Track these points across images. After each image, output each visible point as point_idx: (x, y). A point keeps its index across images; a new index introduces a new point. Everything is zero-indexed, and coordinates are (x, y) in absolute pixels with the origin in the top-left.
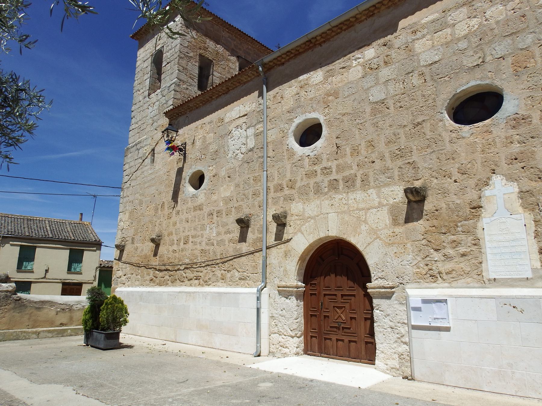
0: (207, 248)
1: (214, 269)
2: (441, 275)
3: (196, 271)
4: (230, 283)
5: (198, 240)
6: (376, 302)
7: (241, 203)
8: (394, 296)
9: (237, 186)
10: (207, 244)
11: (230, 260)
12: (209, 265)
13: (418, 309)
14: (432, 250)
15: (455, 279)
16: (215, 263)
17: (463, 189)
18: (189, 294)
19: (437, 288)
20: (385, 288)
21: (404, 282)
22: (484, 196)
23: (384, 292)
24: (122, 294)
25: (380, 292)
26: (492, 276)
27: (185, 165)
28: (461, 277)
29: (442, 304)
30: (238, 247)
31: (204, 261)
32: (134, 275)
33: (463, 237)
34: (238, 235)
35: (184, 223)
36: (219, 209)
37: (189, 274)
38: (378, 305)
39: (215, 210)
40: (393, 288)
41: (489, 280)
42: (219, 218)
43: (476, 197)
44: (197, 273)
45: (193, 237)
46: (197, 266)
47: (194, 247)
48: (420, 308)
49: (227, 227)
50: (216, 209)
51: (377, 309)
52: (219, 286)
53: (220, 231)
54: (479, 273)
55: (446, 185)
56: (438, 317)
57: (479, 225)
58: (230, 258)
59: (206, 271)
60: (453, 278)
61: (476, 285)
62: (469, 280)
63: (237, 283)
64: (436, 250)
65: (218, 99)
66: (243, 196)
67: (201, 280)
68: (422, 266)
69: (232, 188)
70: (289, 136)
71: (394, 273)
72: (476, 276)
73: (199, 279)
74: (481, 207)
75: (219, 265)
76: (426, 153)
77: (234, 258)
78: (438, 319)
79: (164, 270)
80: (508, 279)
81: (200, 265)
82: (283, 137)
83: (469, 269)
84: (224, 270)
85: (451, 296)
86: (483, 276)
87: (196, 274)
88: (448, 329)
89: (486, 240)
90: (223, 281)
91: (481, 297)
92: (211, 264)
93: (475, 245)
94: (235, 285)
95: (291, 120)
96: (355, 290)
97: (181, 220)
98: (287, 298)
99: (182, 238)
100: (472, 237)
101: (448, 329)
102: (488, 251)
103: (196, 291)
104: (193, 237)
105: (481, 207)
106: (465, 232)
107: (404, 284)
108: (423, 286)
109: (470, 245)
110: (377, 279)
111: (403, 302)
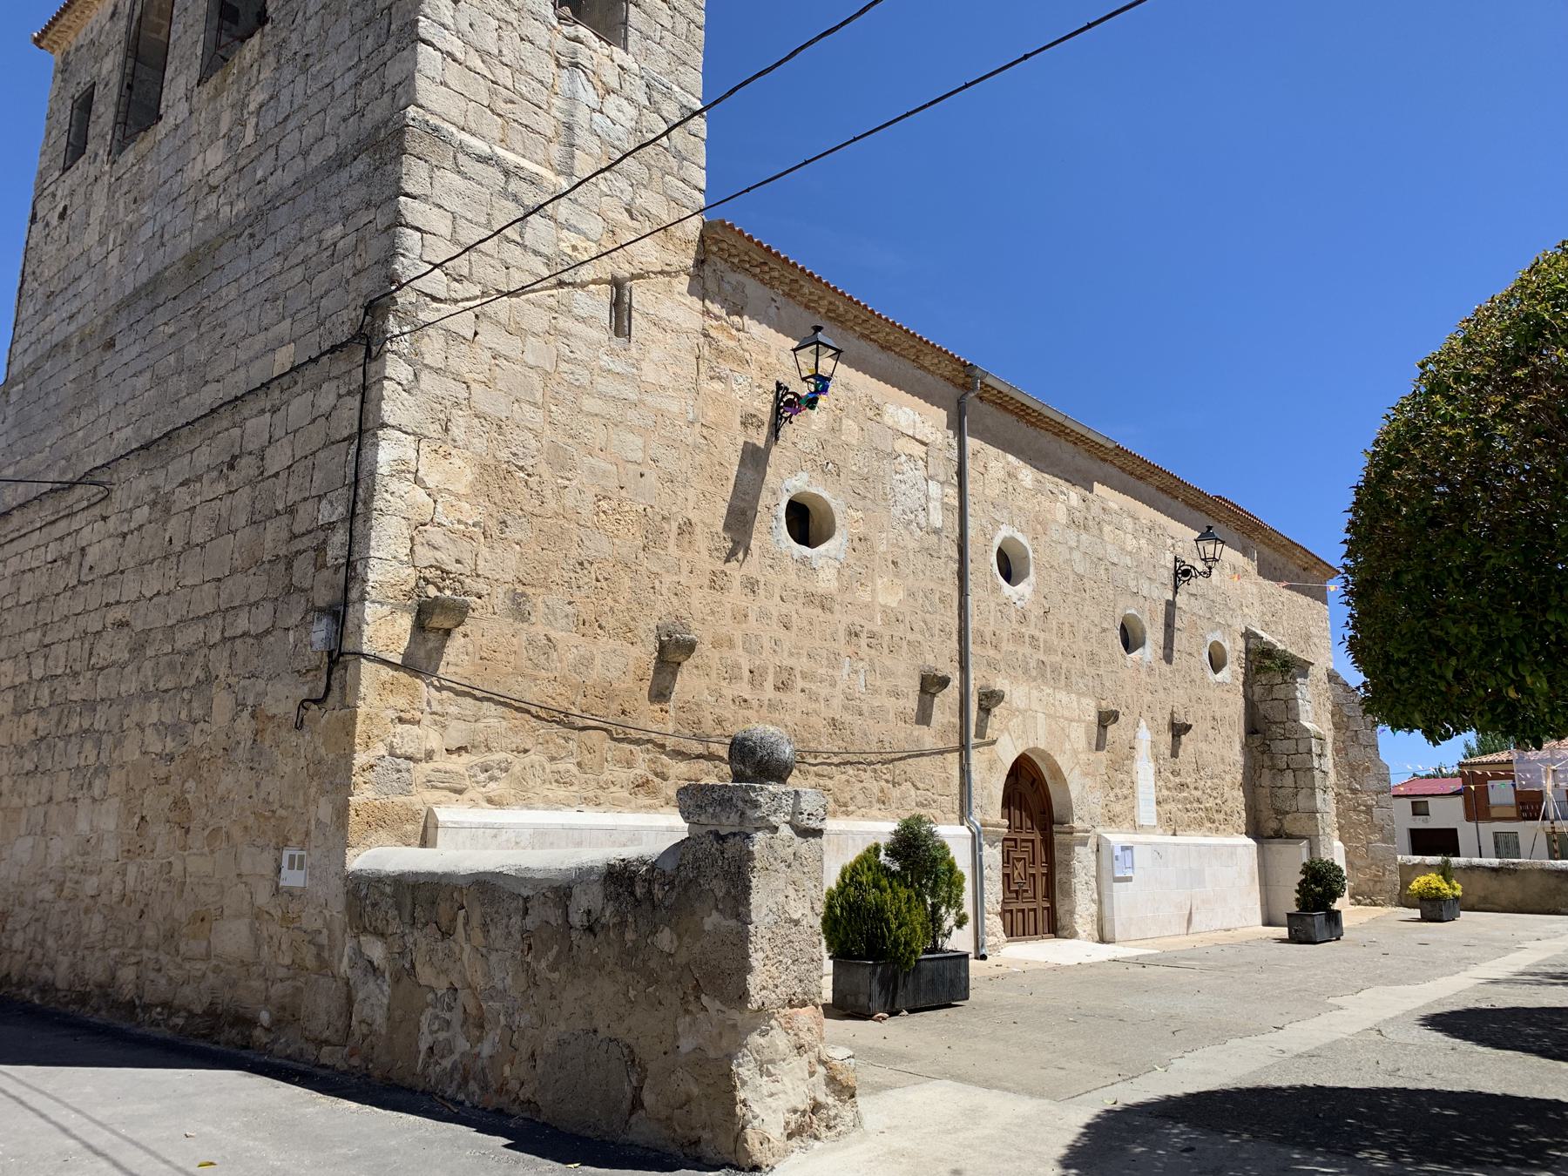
3: (817, 775)
9: (912, 594)
11: (900, 759)
12: (851, 764)
24: (495, 836)
27: (774, 450)
30: (916, 733)
32: (532, 757)
34: (916, 708)
35: (775, 627)
45: (804, 676)
46: (818, 761)
47: (812, 706)
52: (875, 819)
58: (900, 755)
65: (863, 343)
77: (910, 757)
79: (699, 757)
84: (887, 781)
88: (1129, 879)
97: (764, 615)
99: (771, 671)
101: (1129, 879)
104: (804, 676)
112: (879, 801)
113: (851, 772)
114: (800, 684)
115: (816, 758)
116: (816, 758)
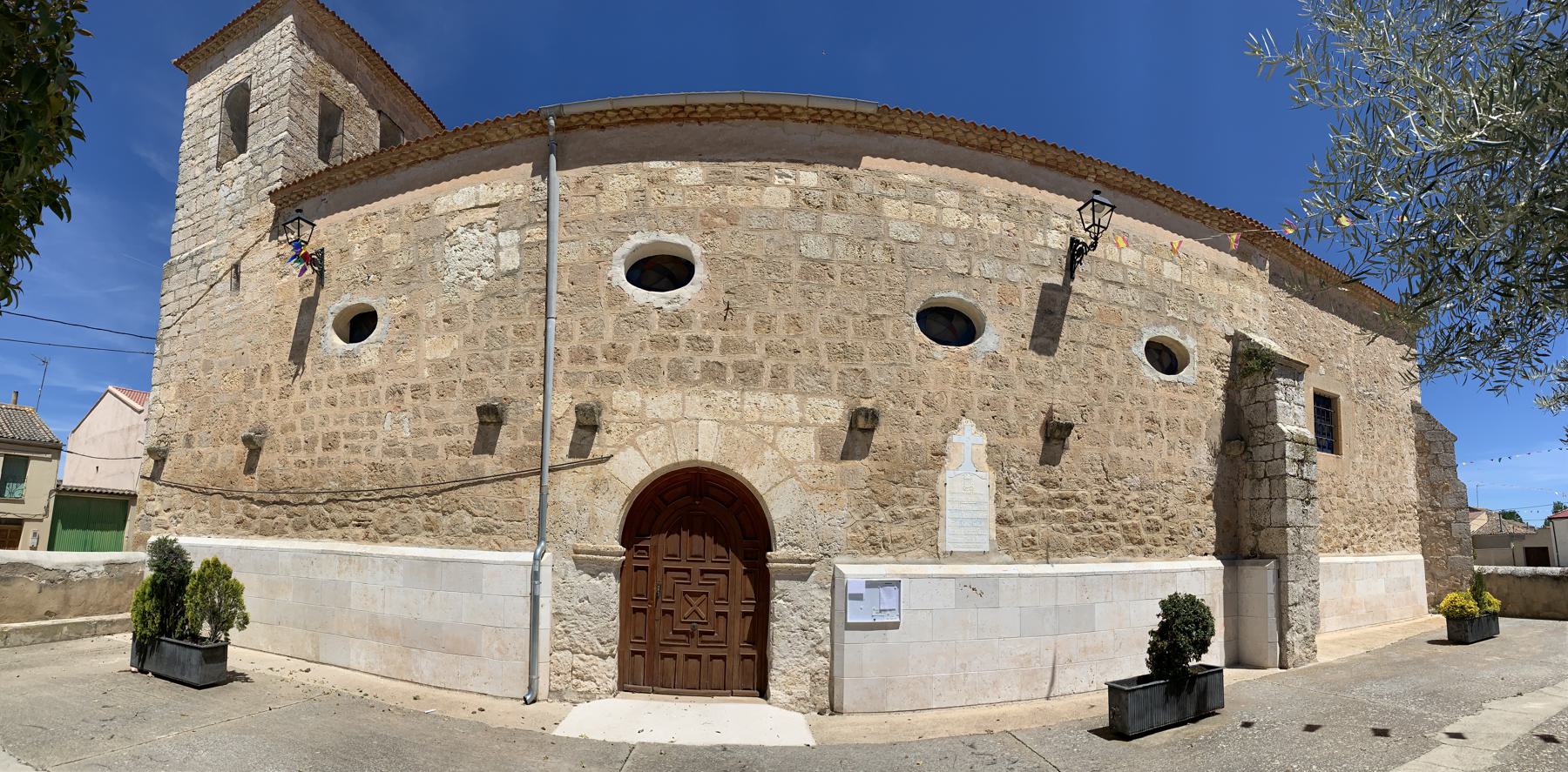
0: (388, 460)
1: (406, 507)
2: (886, 543)
3: (359, 509)
4: (449, 538)
5: (365, 443)
6: (779, 585)
7: (480, 374)
8: (813, 575)
9: (471, 339)
10: (387, 453)
12: (392, 498)
13: (858, 597)
14: (877, 506)
15: (903, 550)
16: (408, 493)
17: (927, 427)
18: (347, 557)
19: (880, 563)
20: (800, 561)
21: (831, 552)
22: (951, 441)
23: (800, 568)
25: (790, 569)
26: (949, 550)
28: (911, 548)
29: (892, 588)
31: (378, 487)
33: (919, 491)
36: (419, 383)
37: (339, 512)
38: (782, 590)
39: (409, 385)
40: (812, 562)
41: (945, 553)
42: (418, 401)
43: (940, 440)
44: (359, 512)
46: (361, 498)
47: (352, 457)
48: (862, 595)
49: (442, 421)
50: (411, 382)
51: (780, 598)
52: (420, 545)
53: (423, 427)
54: (933, 543)
55: (906, 416)
56: (887, 608)
57: (941, 478)
59: (384, 510)
60: (901, 549)
61: (929, 560)
62: (922, 551)
63: (468, 538)
64: (883, 506)
66: (486, 361)
67: (371, 529)
68: (860, 528)
69: (456, 344)
70: (614, 262)
71: (816, 537)
72: (928, 548)
73: (366, 526)
74: (945, 455)
75: (421, 498)
76: (883, 362)
78: (885, 610)
80: (966, 552)
81: (370, 495)
82: (598, 262)
83: (921, 537)
85: (904, 576)
86: (937, 547)
87: (355, 514)
89: (947, 499)
90: (430, 533)
91: (941, 577)
92: (397, 494)
93: (932, 504)
94: (464, 544)
95: (623, 236)
96: (728, 562)
98: (593, 576)
100: (930, 493)
102: (948, 514)
103: (363, 551)
105: (945, 455)
106: (922, 484)
107: (830, 557)
108: (860, 560)
109: (926, 502)
110: (785, 545)
111: (827, 586)
112: (426, 528)
113: (392, 505)
114: (343, 441)
115: (359, 496)
116: (359, 496)
